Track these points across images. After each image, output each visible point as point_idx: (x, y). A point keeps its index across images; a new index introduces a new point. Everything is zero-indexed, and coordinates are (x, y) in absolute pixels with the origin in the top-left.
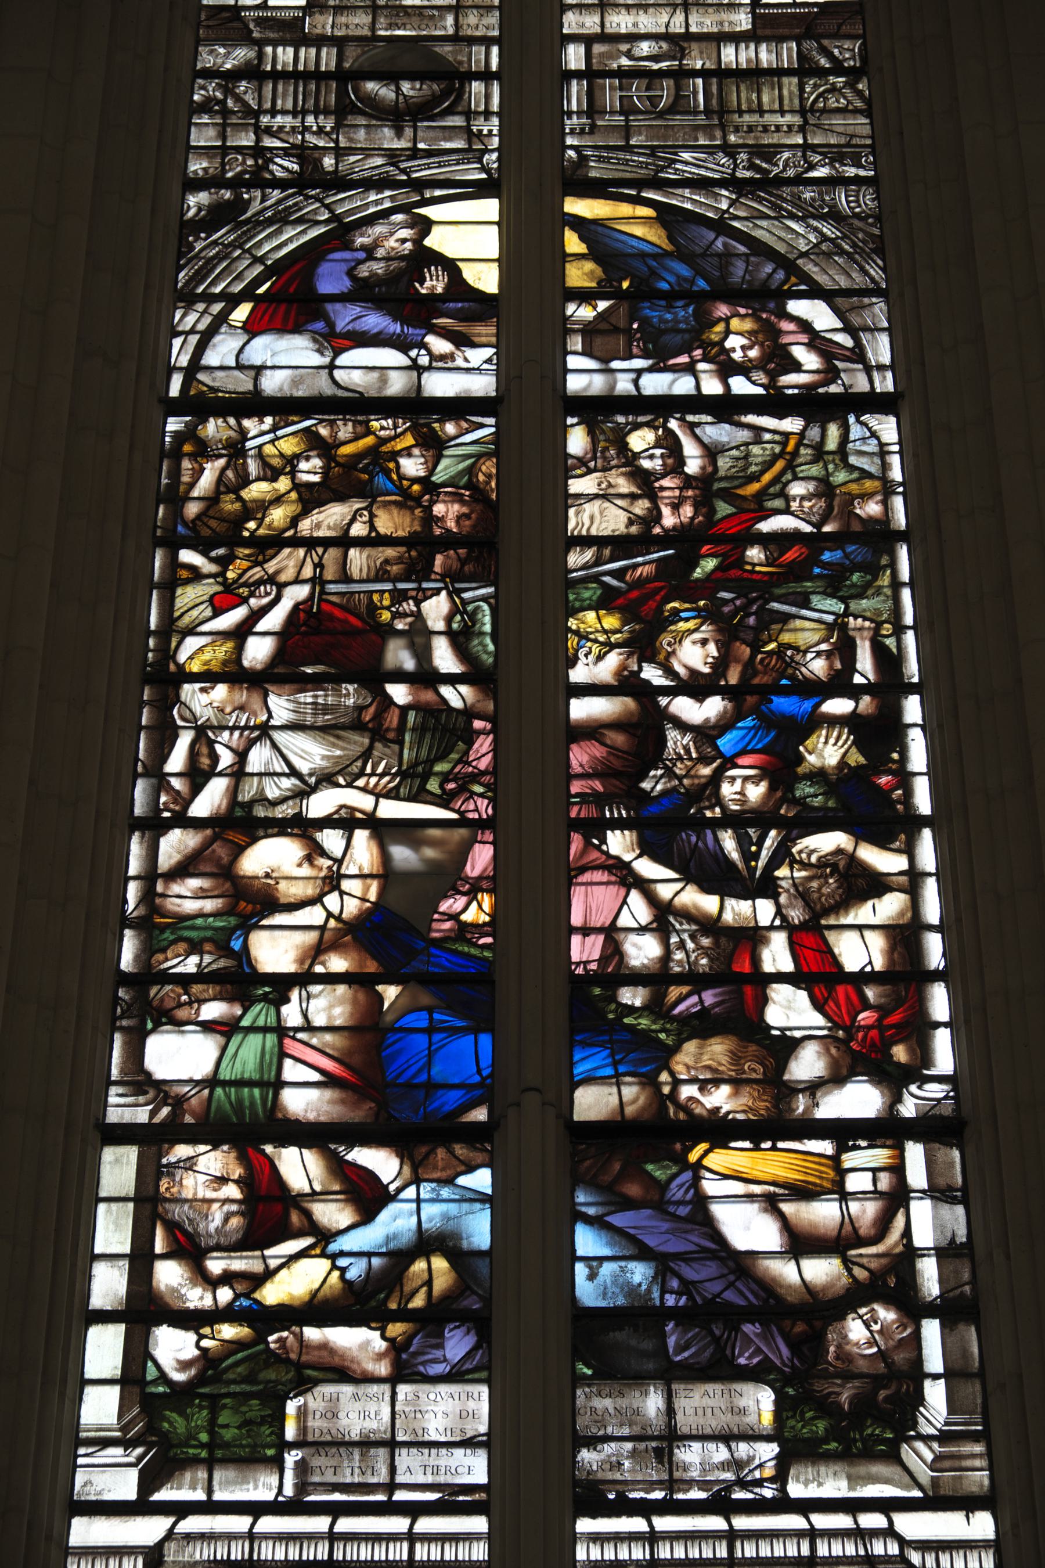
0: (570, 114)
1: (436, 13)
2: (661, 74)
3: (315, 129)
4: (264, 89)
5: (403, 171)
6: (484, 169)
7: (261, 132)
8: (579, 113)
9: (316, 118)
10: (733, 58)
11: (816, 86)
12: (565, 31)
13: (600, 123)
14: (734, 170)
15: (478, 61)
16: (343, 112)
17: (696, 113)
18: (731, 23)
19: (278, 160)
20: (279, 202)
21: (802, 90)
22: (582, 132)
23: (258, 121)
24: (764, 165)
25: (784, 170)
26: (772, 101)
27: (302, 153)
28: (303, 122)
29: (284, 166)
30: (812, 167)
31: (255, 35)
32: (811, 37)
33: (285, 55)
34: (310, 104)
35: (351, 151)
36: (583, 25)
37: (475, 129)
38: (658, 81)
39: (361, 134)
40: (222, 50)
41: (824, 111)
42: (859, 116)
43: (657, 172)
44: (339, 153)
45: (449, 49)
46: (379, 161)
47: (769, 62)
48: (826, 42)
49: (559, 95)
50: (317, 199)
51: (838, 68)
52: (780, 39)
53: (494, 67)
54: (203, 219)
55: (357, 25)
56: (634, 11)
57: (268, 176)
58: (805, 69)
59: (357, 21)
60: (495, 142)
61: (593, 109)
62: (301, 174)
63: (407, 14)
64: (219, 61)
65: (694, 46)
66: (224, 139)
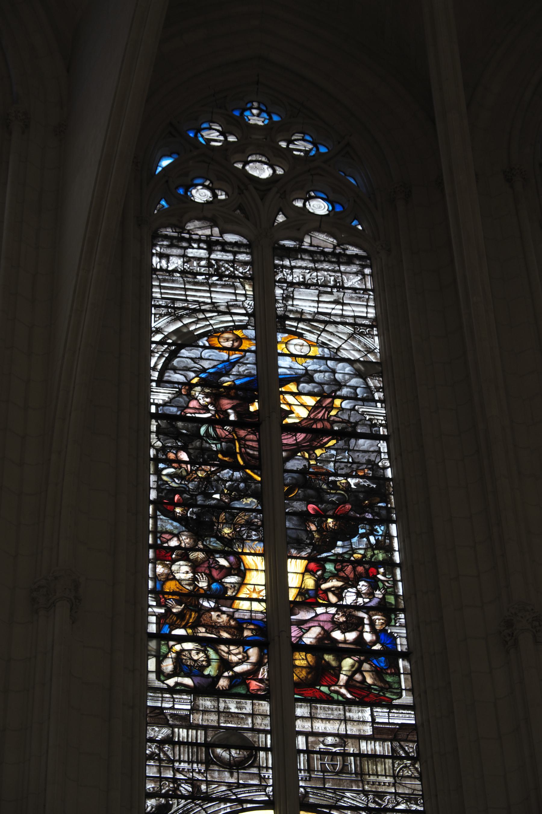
0: (300, 770)
1: (244, 716)
2: (336, 754)
3: (197, 770)
4: (175, 749)
5: (234, 794)
6: (267, 795)
7: (176, 770)
8: (304, 770)
9: (197, 765)
10: (365, 748)
11: (399, 764)
12: (297, 729)
13: (313, 776)
14: (368, 802)
15: (262, 742)
16: (208, 762)
17: (351, 774)
18: (364, 731)
19: (183, 785)
20: (185, 806)
21: (393, 766)
22: (306, 780)
23: (174, 765)
24: (380, 801)
25: (387, 804)
26: (382, 771)
27: (192, 782)
28: (192, 767)
29: (185, 789)
30: (398, 804)
31: (170, 722)
32: (396, 740)
33: (183, 733)
34: (195, 759)
35: (213, 782)
36: (304, 727)
37: (262, 775)
38: (335, 757)
39: (216, 774)
40: (157, 729)
41: (403, 777)
42: (416, 780)
43: (337, 801)
44: (208, 783)
45: (250, 734)
46: (224, 788)
47: (380, 752)
48: (402, 743)
49: (295, 762)
50: (201, 806)
51: (408, 757)
52: (384, 740)
53: (269, 746)
54: (153, 812)
55: (212, 720)
56: (324, 722)
57: (179, 793)
58: (394, 756)
59: (212, 718)
60: (271, 782)
61: (310, 769)
62: (193, 792)
63: (232, 716)
64: (156, 734)
65: (350, 741)
66: (160, 774)
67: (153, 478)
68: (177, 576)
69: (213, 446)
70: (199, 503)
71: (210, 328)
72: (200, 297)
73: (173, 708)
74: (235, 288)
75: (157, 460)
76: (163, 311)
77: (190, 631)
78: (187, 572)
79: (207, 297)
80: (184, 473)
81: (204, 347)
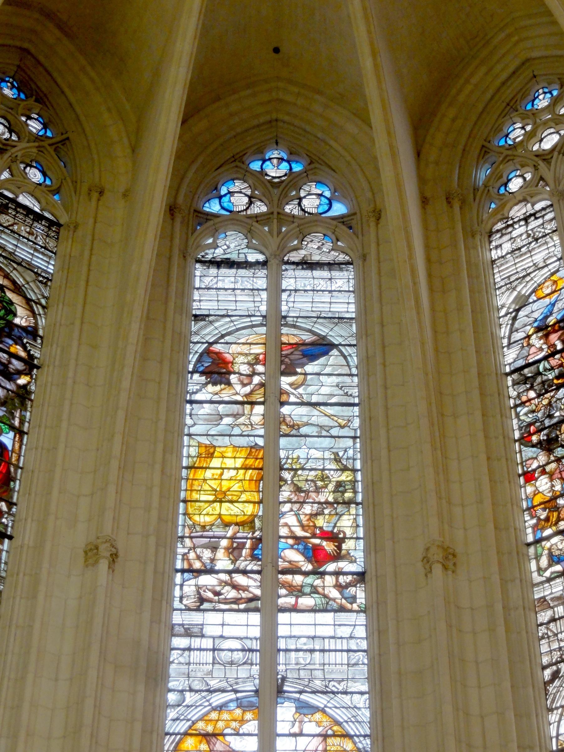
31: (551, 605)
67: (515, 421)
68: (541, 490)
69: (550, 376)
70: (546, 425)
71: (536, 284)
72: (525, 264)
73: (552, 593)
74: (546, 243)
75: (516, 406)
76: (504, 289)
77: (554, 528)
78: (547, 483)
79: (530, 262)
80: (534, 407)
81: (534, 302)
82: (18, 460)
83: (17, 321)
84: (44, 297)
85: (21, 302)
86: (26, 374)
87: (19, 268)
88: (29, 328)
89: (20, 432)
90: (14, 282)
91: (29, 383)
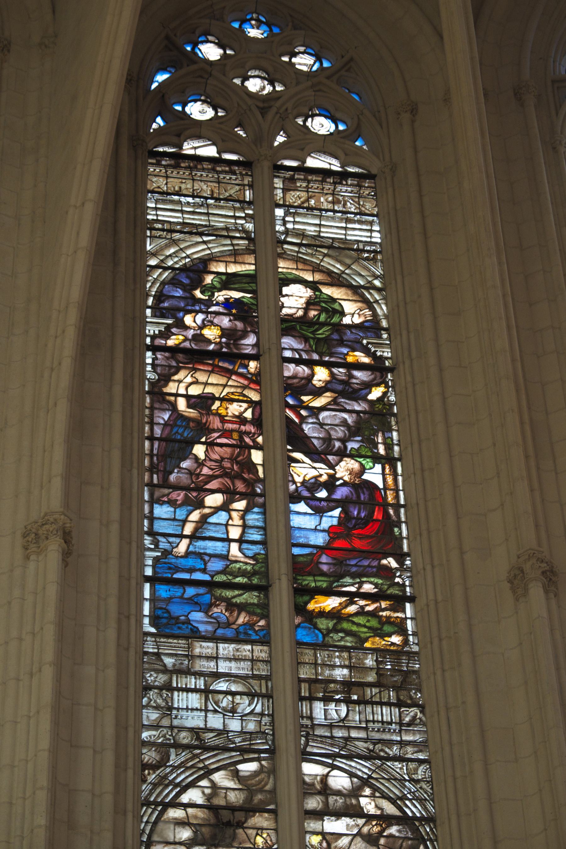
82: (397, 497)
83: (347, 320)
84: (376, 277)
85: (347, 294)
86: (378, 385)
87: (331, 252)
88: (366, 324)
89: (388, 461)
90: (329, 273)
91: (385, 394)
